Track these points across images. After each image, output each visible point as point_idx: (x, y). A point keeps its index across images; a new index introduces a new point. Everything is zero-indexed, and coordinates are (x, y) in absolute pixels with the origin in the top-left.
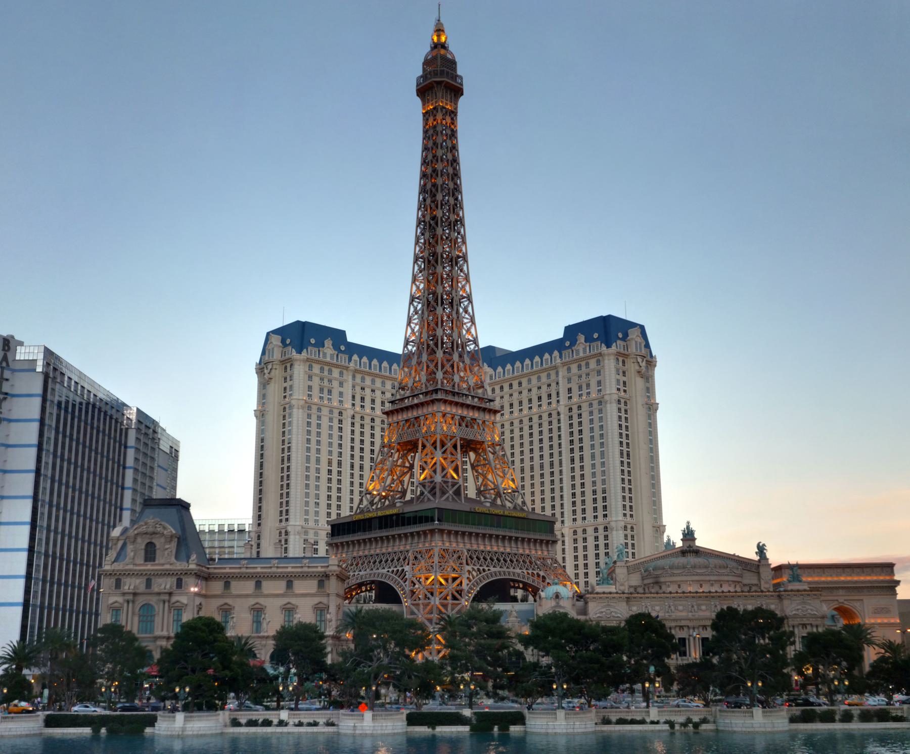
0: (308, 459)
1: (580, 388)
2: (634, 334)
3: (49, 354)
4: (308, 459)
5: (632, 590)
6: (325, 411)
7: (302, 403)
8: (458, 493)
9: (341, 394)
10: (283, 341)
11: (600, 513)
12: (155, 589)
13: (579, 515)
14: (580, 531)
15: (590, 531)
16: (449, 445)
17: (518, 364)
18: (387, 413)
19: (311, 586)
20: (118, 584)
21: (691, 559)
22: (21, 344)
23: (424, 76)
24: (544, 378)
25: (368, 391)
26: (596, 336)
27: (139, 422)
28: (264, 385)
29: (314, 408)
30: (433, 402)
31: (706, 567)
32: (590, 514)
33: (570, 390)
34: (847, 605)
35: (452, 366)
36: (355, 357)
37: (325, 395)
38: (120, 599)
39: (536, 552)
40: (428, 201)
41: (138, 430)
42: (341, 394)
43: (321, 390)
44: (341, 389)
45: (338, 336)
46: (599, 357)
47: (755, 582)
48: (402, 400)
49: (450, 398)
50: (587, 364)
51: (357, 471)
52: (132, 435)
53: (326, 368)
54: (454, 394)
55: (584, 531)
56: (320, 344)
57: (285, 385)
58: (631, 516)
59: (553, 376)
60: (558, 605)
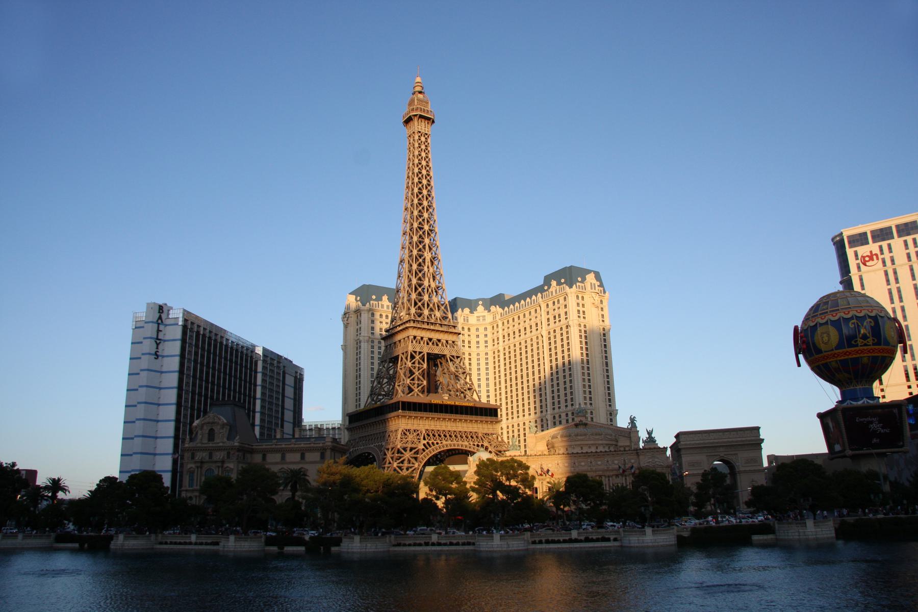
1: (555, 317)
2: (590, 278)
3: (186, 313)
7: (366, 338)
11: (569, 403)
12: (215, 459)
13: (556, 406)
14: (557, 416)
15: (563, 415)
16: (417, 357)
19: (316, 456)
22: (172, 308)
26: (563, 281)
27: (264, 356)
31: (585, 435)
32: (563, 404)
33: (548, 319)
34: (726, 458)
38: (193, 466)
41: (264, 361)
47: (628, 444)
52: (260, 364)
55: (560, 416)
58: (591, 404)
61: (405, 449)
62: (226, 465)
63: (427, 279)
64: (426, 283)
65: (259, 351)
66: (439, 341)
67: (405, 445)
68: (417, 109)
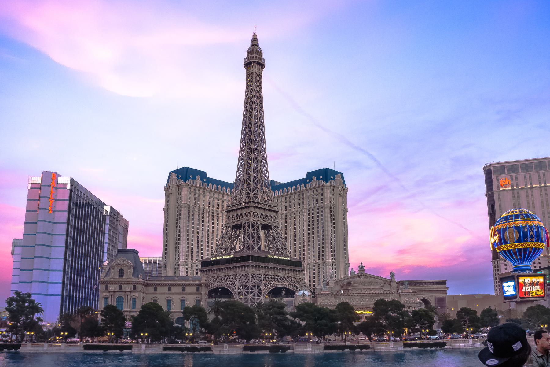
0: (188, 231)
1: (313, 201)
2: (338, 177)
4: (188, 231)
5: (336, 292)
6: (196, 209)
8: (260, 248)
9: (204, 201)
10: (177, 177)
11: (321, 258)
13: (312, 258)
15: (316, 266)
16: (256, 226)
17: (285, 189)
18: (227, 212)
19: (194, 289)
20: (107, 288)
21: (362, 279)
22: (60, 176)
23: (247, 59)
24: (297, 196)
25: (216, 200)
26: (321, 177)
27: (111, 212)
28: (168, 196)
29: (191, 208)
30: (249, 207)
35: (258, 191)
36: (210, 184)
37: (196, 202)
38: (108, 294)
39: (293, 275)
40: (248, 114)
41: (111, 216)
42: (204, 201)
43: (195, 199)
44: (204, 199)
45: (203, 174)
46: (322, 187)
48: (234, 206)
49: (256, 205)
50: (317, 190)
51: (210, 238)
53: (197, 189)
54: (258, 203)
56: (194, 178)
57: (178, 196)
59: (301, 196)
60: (304, 299)
61: (254, 286)
62: (132, 294)
63: (260, 174)
64: (259, 177)
65: (107, 208)
66: (267, 216)
67: (254, 285)
68: (256, 57)
